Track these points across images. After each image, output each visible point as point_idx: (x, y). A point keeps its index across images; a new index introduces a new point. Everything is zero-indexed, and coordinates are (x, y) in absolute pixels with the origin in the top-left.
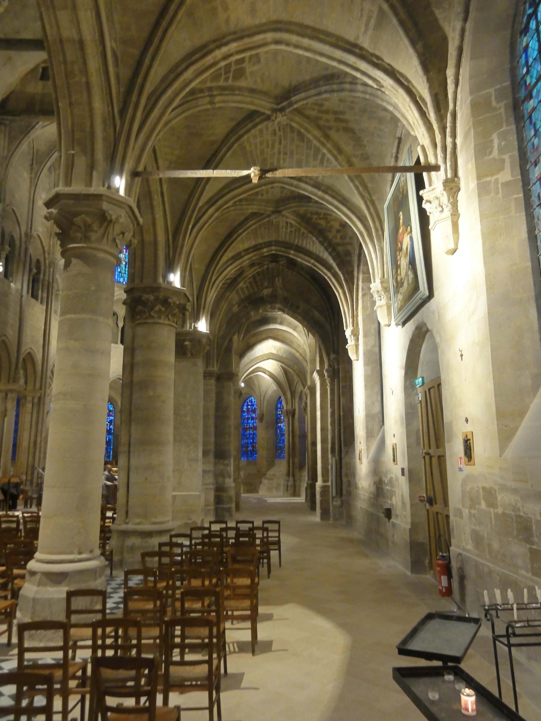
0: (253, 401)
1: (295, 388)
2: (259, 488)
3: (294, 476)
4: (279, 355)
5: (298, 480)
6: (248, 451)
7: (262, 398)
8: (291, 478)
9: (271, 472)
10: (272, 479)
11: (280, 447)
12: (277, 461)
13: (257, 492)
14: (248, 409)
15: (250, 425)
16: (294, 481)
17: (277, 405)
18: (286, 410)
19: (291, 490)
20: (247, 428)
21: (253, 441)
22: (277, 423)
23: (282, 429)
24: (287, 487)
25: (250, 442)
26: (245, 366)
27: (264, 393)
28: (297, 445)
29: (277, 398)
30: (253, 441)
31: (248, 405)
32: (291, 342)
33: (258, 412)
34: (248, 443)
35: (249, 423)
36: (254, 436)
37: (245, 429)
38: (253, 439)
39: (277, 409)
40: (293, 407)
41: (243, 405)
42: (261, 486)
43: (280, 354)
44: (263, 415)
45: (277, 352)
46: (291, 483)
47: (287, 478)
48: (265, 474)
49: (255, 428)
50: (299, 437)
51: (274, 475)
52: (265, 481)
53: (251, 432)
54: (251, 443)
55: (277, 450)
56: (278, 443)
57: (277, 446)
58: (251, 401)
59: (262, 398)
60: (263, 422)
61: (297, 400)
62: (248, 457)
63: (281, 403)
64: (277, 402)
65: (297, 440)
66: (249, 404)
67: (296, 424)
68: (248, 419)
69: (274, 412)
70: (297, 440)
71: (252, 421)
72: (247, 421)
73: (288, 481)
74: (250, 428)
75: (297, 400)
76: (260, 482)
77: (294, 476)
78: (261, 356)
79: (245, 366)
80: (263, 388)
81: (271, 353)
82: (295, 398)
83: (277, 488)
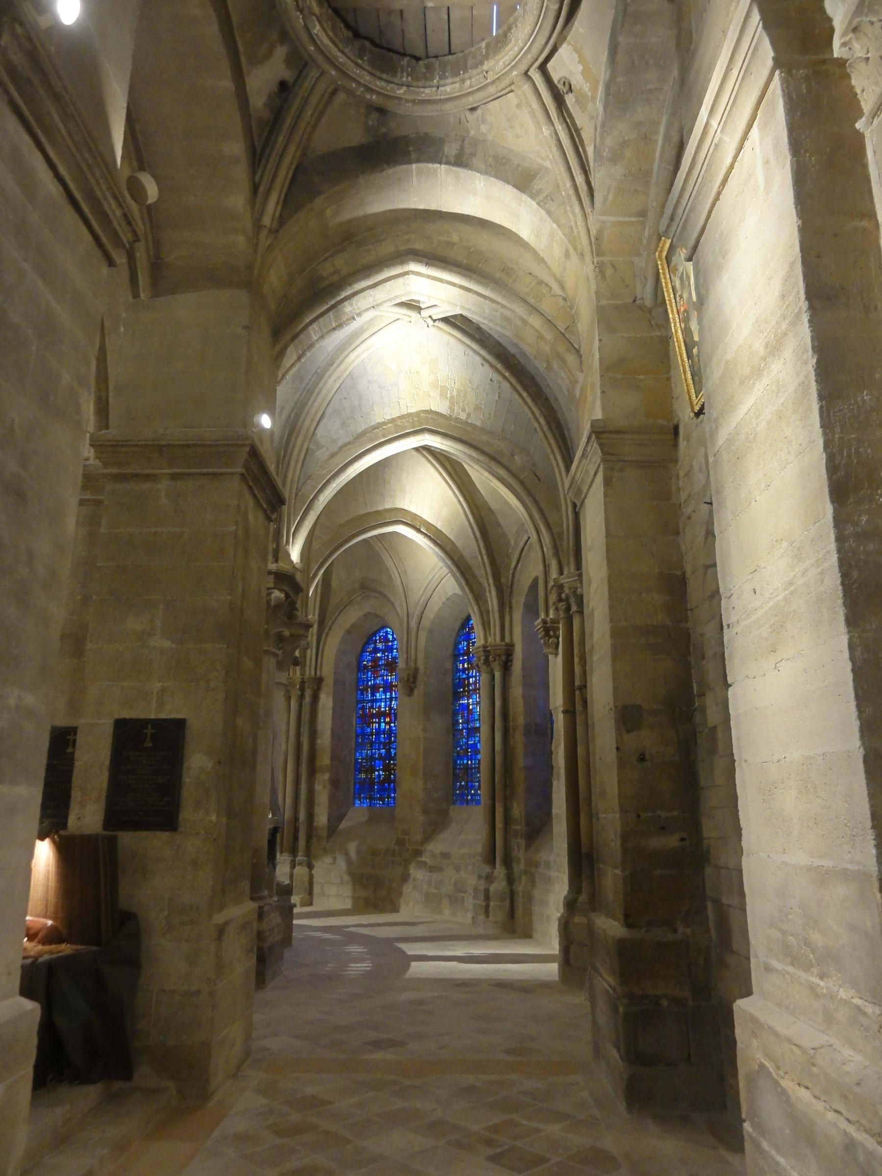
0: (390, 637)
1: (513, 577)
2: (400, 894)
3: (508, 862)
4: (457, 420)
5: (524, 878)
6: (372, 783)
7: (413, 624)
8: (500, 871)
9: (436, 847)
10: (439, 869)
11: (467, 768)
12: (457, 812)
13: (395, 910)
14: (375, 660)
15: (380, 707)
16: (510, 879)
17: (457, 644)
18: (485, 647)
19: (498, 914)
20: (373, 716)
21: (388, 752)
22: (457, 696)
23: (470, 712)
24: (487, 898)
25: (380, 754)
26: (333, 455)
27: (419, 609)
28: (520, 761)
29: (458, 624)
30: (388, 752)
31: (376, 650)
32: (507, 270)
33: (401, 664)
34: (372, 758)
35: (376, 701)
36: (390, 737)
37: (366, 719)
38: (388, 745)
39: (456, 656)
40: (507, 640)
41: (363, 650)
42: (407, 889)
43: (463, 416)
44: (416, 670)
45: (451, 408)
46: (499, 886)
47: (487, 869)
48: (418, 853)
49: (392, 714)
50: (527, 732)
51: (446, 856)
52: (418, 874)
53: (383, 725)
54: (381, 757)
55: (456, 778)
56: (459, 757)
57: (455, 763)
58: (385, 639)
59: (413, 624)
60: (416, 692)
61: (518, 615)
62: (371, 798)
63: (468, 638)
64: (458, 635)
65: (519, 740)
66: (380, 646)
67: (517, 691)
68: (375, 689)
69: (448, 665)
70: (519, 740)
71: (385, 692)
72: (373, 695)
73: (489, 878)
74: (381, 715)
75: (518, 615)
76: (405, 878)
77: (508, 862)
78: (392, 421)
79: (333, 455)
80: (417, 594)
81: (430, 412)
82: (511, 608)
83: (455, 900)
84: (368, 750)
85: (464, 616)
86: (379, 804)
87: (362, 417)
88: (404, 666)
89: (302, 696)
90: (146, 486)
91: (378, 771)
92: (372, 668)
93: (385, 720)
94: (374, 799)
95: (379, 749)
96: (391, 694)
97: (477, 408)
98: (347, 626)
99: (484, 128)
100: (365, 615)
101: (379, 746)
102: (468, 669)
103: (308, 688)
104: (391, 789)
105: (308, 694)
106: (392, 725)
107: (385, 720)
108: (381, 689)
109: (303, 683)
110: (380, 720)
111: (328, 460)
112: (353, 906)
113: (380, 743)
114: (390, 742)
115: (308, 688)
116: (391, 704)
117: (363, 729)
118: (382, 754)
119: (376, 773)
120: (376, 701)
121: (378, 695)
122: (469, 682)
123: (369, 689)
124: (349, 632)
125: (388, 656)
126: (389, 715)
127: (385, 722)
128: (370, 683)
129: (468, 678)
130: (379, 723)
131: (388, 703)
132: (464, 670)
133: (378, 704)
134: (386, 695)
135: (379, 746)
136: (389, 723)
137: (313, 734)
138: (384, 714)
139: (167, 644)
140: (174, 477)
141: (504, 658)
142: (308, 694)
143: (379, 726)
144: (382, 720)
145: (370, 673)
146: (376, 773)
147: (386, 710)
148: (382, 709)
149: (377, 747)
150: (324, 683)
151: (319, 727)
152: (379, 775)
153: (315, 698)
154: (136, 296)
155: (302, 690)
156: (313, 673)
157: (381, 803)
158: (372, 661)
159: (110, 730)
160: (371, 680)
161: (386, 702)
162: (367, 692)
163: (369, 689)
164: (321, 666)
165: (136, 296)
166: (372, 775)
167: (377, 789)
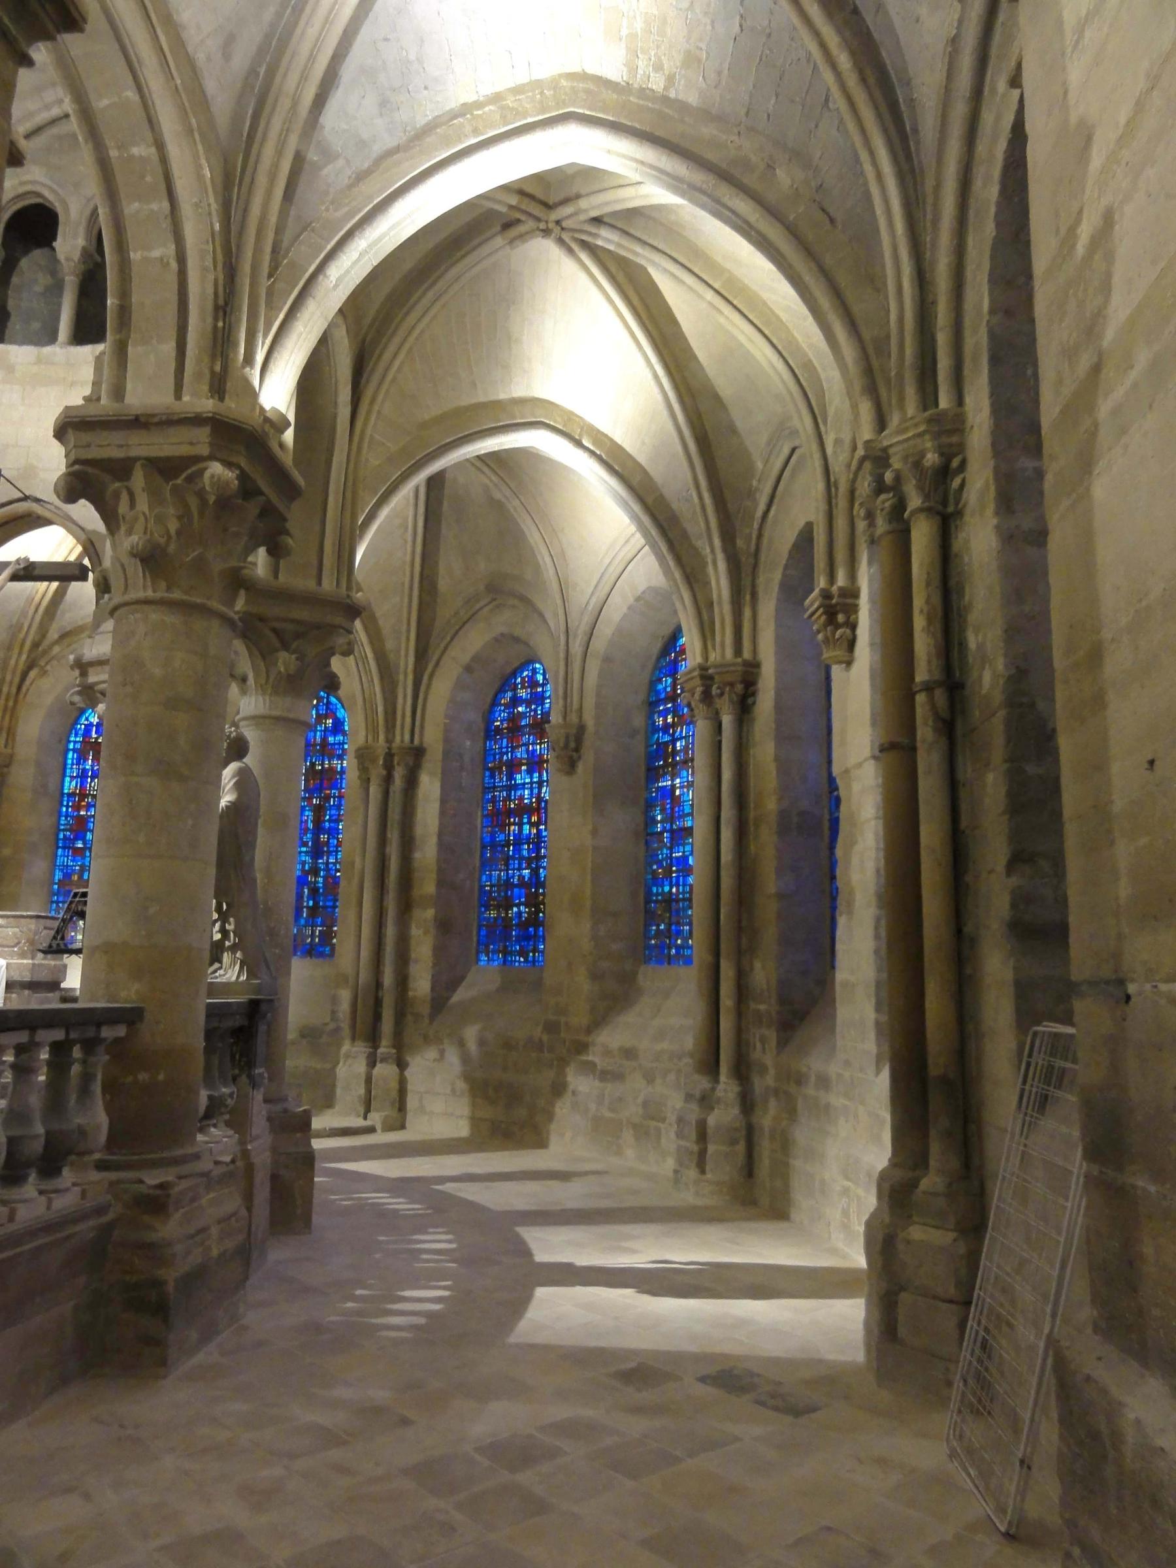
0: (540, 678)
1: (760, 536)
2: (550, 1117)
3: (743, 1070)
4: (643, 92)
5: (772, 1103)
6: (507, 925)
7: (577, 648)
8: (727, 1087)
9: (611, 1037)
10: (616, 1076)
11: (669, 900)
12: (651, 976)
13: (541, 1143)
14: (514, 719)
15: (522, 798)
16: (747, 1103)
17: (654, 682)
18: (703, 668)
19: (723, 1168)
20: (510, 813)
21: (535, 872)
22: (653, 774)
23: (676, 801)
24: (702, 1135)
25: (521, 877)
26: (361, 177)
27: (587, 619)
28: (770, 882)
29: (657, 646)
30: (535, 872)
31: (516, 701)
33: (555, 718)
34: (508, 884)
35: (516, 787)
36: (538, 848)
37: (499, 817)
38: (535, 862)
39: (652, 705)
40: (747, 655)
41: (495, 703)
42: (562, 1109)
43: (657, 83)
44: (582, 728)
46: (725, 1115)
47: (703, 1083)
48: (581, 1047)
49: (539, 808)
50: (784, 826)
51: (629, 1053)
52: (580, 1084)
53: (526, 828)
54: (522, 883)
55: (650, 917)
56: (656, 881)
57: (649, 893)
58: (533, 683)
59: (577, 648)
60: (580, 767)
61: (768, 607)
62: (506, 953)
63: (673, 670)
64: (657, 667)
65: (766, 843)
66: (523, 693)
67: (764, 751)
68: (513, 767)
69: (639, 721)
70: (766, 843)
71: (530, 772)
72: (511, 777)
73: (706, 1101)
74: (524, 810)
75: (768, 607)
76: (559, 1089)
77: (743, 1070)
78: (496, 98)
79: (361, 177)
80: (584, 593)
81: (584, 76)
82: (754, 595)
83: (643, 1132)
84: (500, 871)
85: (667, 631)
86: (520, 962)
87: (426, 88)
88: (560, 720)
89: (388, 779)
91: (518, 905)
92: (508, 733)
93: (529, 818)
94: (511, 953)
95: (520, 869)
96: (540, 776)
97: (690, 60)
98: (466, 658)
100: (496, 640)
101: (520, 864)
102: (673, 725)
103: (398, 764)
104: (540, 937)
105: (399, 774)
106: (542, 827)
107: (529, 818)
109: (389, 756)
110: (521, 819)
111: (350, 187)
112: (472, 1134)
113: (522, 858)
114: (539, 858)
115: (398, 764)
116: (540, 792)
117: (493, 837)
118: (524, 877)
119: (515, 909)
120: (516, 787)
121: (518, 776)
123: (504, 768)
124: (468, 669)
125: (535, 710)
127: (529, 822)
129: (674, 742)
130: (521, 825)
131: (536, 791)
132: (666, 728)
133: (519, 793)
134: (531, 778)
135: (520, 864)
136: (536, 825)
137: (408, 843)
138: (529, 810)
141: (739, 688)
142: (399, 774)
143: (521, 830)
144: (525, 820)
145: (505, 741)
146: (515, 909)
147: (531, 803)
149: (516, 866)
150: (428, 757)
151: (419, 831)
152: (520, 913)
153: (411, 782)
155: (389, 767)
156: (407, 737)
157: (522, 959)
160: (507, 753)
161: (531, 789)
162: (501, 773)
163: (504, 768)
164: (422, 727)
166: (507, 914)
167: (516, 936)
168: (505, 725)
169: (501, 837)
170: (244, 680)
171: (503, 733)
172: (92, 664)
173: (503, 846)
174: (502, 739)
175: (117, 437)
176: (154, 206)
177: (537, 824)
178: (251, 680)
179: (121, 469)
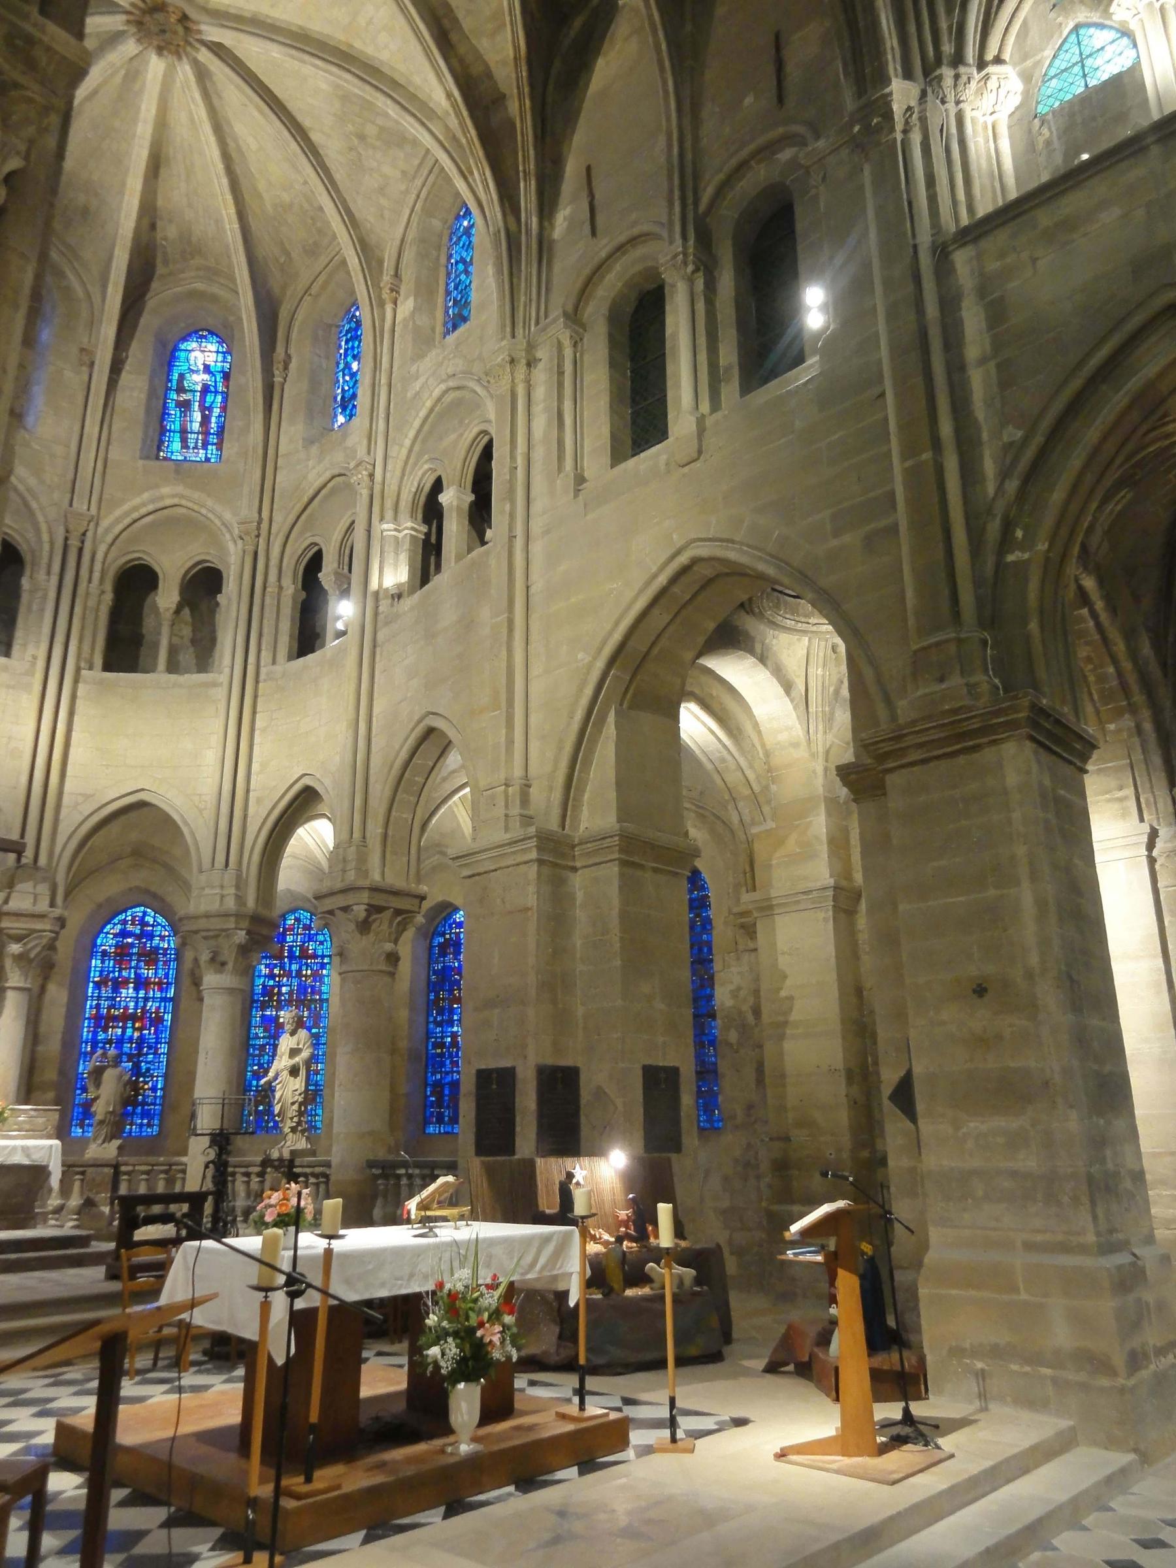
20: (115, 1018)
32: (739, 730)
53: (129, 1032)
71: (136, 989)
90: (639, 873)
92: (115, 956)
93: (133, 1024)
98: (101, 898)
99: (774, 642)
100: (131, 889)
102: (279, 976)
104: (137, 1114)
106: (146, 1032)
107: (133, 1024)
108: (132, 985)
110: (125, 1023)
114: (140, 1054)
116: (145, 1005)
117: (95, 1034)
122: (280, 990)
123: (110, 983)
125: (145, 943)
126: (141, 1019)
128: (111, 975)
129: (280, 987)
130: (124, 1029)
134: (138, 993)
136: (141, 1029)
138: (134, 1018)
139: (662, 1006)
140: (656, 870)
143: (124, 1033)
145: (112, 962)
147: (136, 1013)
148: (131, 1011)
151: (43, 1029)
154: (621, 705)
158: (117, 946)
159: (640, 1073)
160: (113, 972)
161: (137, 1003)
162: (106, 986)
163: (110, 983)
165: (621, 705)
168: (112, 950)
169: (101, 1036)
170: (223, 964)
171: (110, 956)
172: (8, 914)
173: (105, 1043)
174: (109, 960)
175: (384, 896)
176: (412, 798)
177: (141, 1029)
178: (230, 966)
179: (379, 909)
